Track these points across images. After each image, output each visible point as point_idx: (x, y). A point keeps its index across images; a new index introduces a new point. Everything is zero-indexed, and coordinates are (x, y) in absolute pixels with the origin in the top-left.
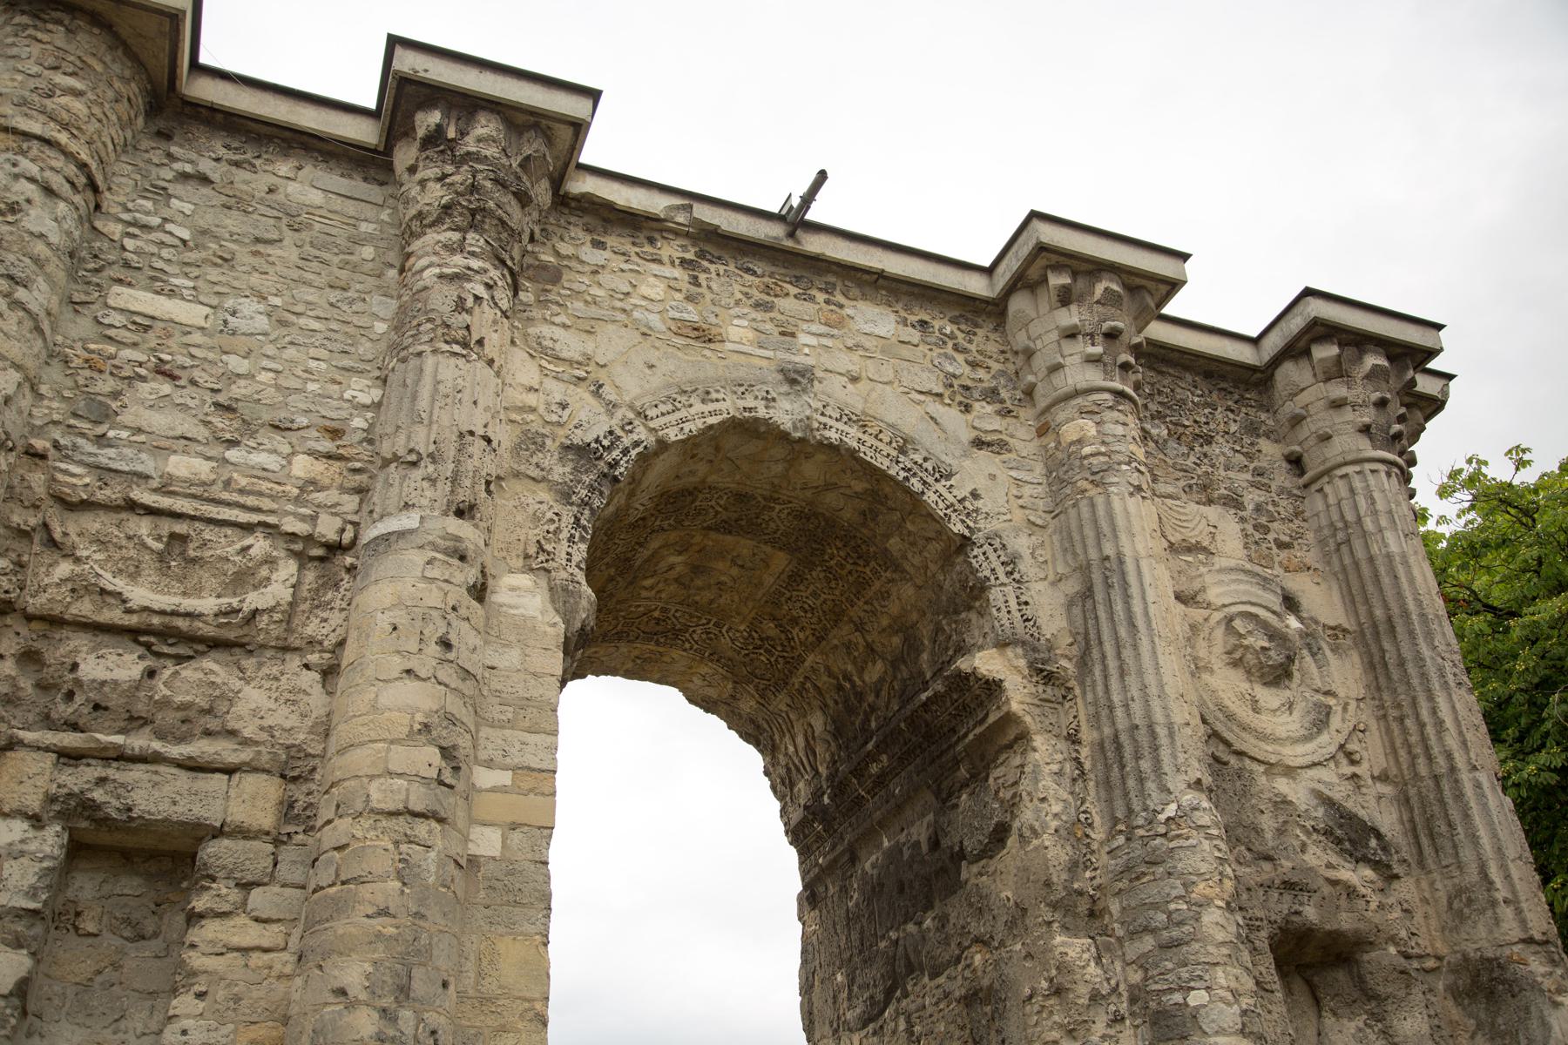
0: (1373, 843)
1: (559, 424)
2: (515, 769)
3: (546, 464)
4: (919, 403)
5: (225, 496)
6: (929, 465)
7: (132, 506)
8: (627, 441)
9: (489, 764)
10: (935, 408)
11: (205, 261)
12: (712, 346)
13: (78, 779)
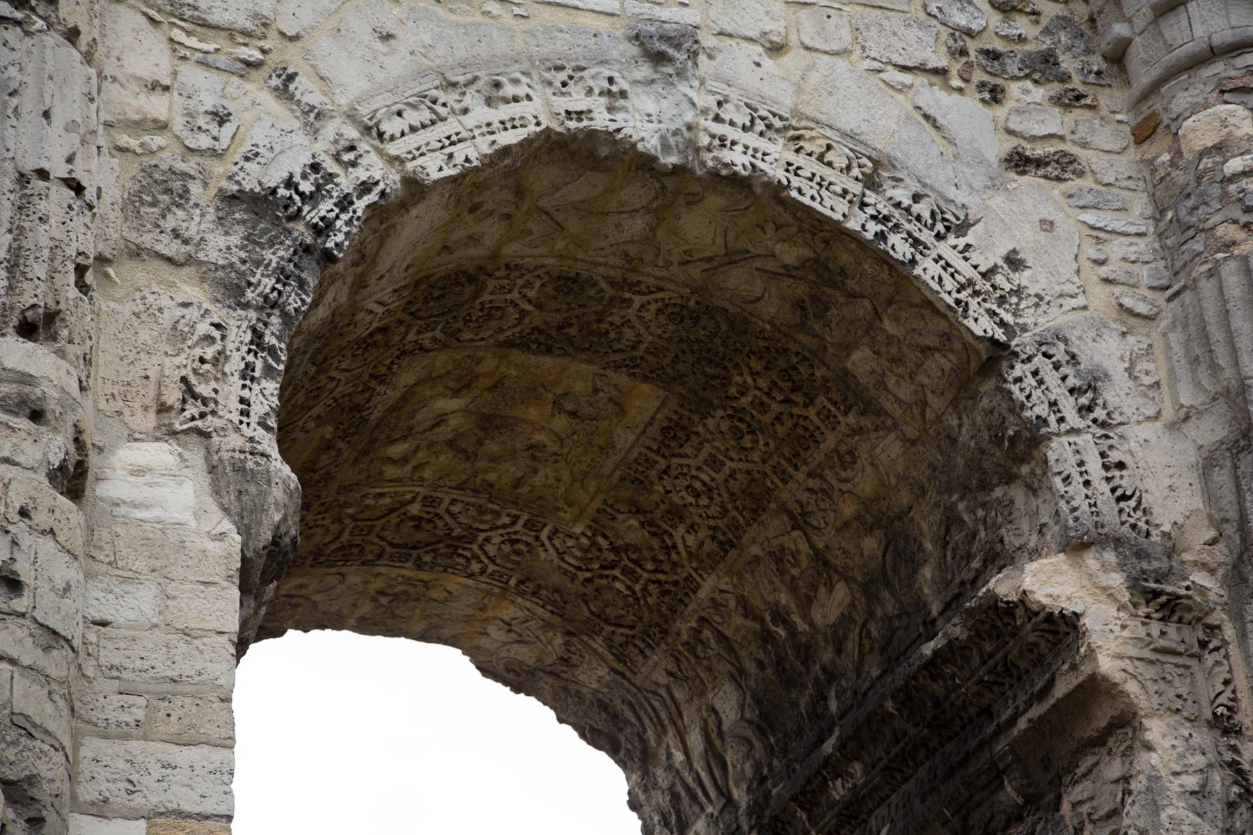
1: (214, 153)
3: (192, 231)
4: (902, 89)
6: (923, 209)
8: (346, 182)
10: (933, 97)
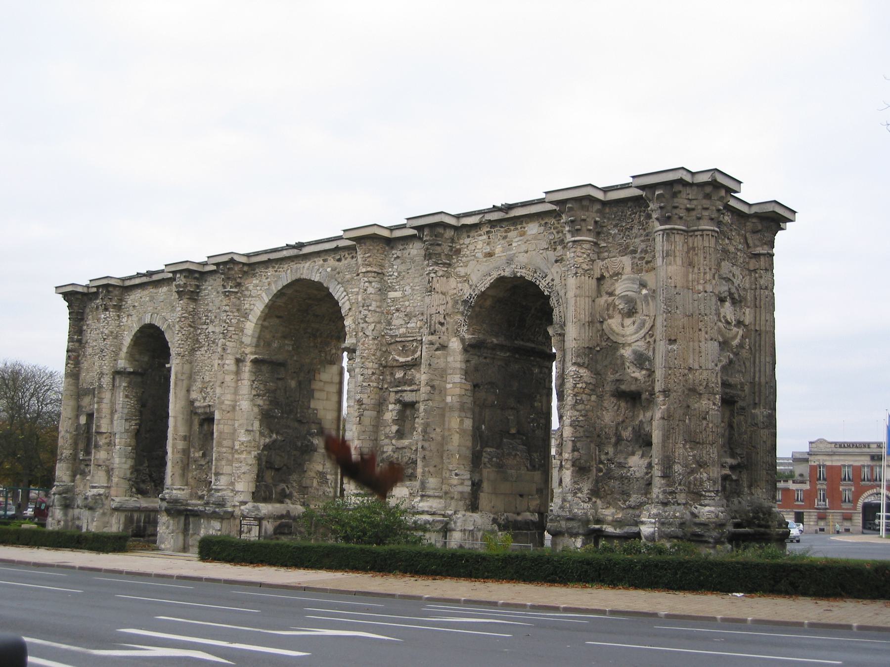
0: (647, 363)
2: (453, 383)
4: (541, 254)
6: (541, 276)
7: (397, 341)
8: (474, 295)
9: (449, 383)
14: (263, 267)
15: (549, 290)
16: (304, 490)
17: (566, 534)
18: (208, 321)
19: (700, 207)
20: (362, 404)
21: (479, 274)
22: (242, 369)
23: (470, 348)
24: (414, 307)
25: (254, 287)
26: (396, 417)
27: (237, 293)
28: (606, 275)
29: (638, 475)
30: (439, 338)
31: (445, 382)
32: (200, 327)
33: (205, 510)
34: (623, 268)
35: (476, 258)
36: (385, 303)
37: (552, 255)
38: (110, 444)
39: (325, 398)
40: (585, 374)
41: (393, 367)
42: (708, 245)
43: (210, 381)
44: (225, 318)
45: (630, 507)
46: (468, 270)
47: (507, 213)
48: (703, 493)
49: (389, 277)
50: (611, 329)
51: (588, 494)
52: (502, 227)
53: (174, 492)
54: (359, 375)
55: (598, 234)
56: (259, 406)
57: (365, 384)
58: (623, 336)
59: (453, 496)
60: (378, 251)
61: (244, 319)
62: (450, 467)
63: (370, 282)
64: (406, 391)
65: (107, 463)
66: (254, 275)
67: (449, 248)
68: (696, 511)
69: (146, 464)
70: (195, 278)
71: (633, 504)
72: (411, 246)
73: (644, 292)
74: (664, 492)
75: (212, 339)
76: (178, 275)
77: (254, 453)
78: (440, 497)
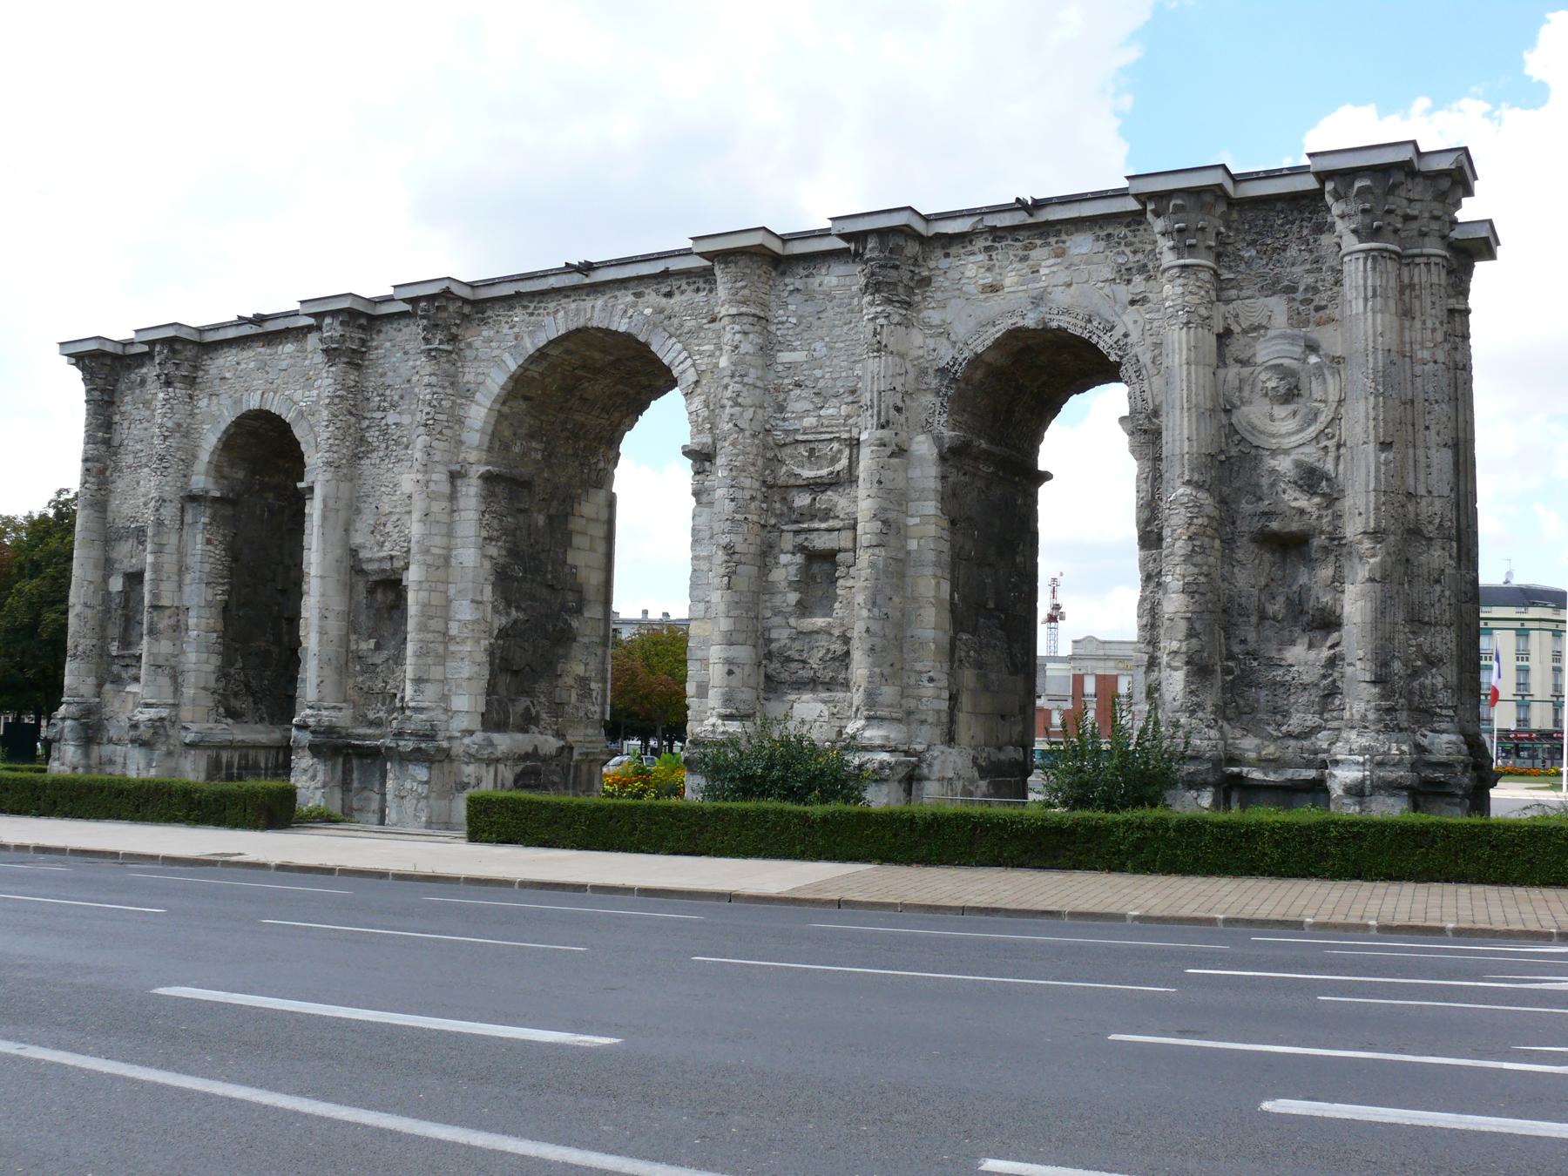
0: (1324, 483)
3: (928, 381)
4: (1101, 288)
5: (822, 430)
6: (1101, 327)
7: (797, 441)
8: (960, 360)
9: (912, 516)
11: (803, 330)
12: (998, 293)
13: (800, 539)
14: (503, 307)
15: (1120, 353)
16: (557, 708)
17: (1180, 785)
18: (386, 404)
19: (1426, 215)
20: (734, 553)
21: (972, 323)
22: (461, 491)
23: (951, 456)
24: (835, 379)
25: (483, 342)
26: (796, 576)
27: (451, 352)
28: (1236, 328)
29: (1306, 679)
30: (896, 434)
31: (906, 513)
32: (369, 415)
33: (398, 746)
34: (1270, 316)
35: (965, 293)
36: (772, 372)
37: (1123, 292)
38: (178, 629)
39: (587, 546)
40: (1207, 502)
41: (787, 487)
42: (1437, 282)
43: (391, 513)
44: (428, 397)
45: (1289, 735)
46: (948, 315)
47: (1031, 215)
48: (1438, 710)
49: (779, 326)
50: (1249, 423)
51: (1212, 713)
52: (1017, 240)
53: (325, 713)
54: (727, 501)
55: (1218, 256)
56: (491, 557)
57: (738, 517)
58: (1273, 436)
59: (924, 717)
60: (759, 277)
61: (463, 401)
62: (919, 666)
63: (746, 333)
64: (817, 530)
65: (173, 662)
66: (484, 322)
67: (910, 274)
68: (1425, 742)
69: (239, 665)
70: (361, 327)
71: (1297, 730)
72: (824, 271)
73: (1313, 359)
74: (1377, 710)
75: (394, 437)
76: (328, 320)
77: (485, 643)
78: (899, 721)
